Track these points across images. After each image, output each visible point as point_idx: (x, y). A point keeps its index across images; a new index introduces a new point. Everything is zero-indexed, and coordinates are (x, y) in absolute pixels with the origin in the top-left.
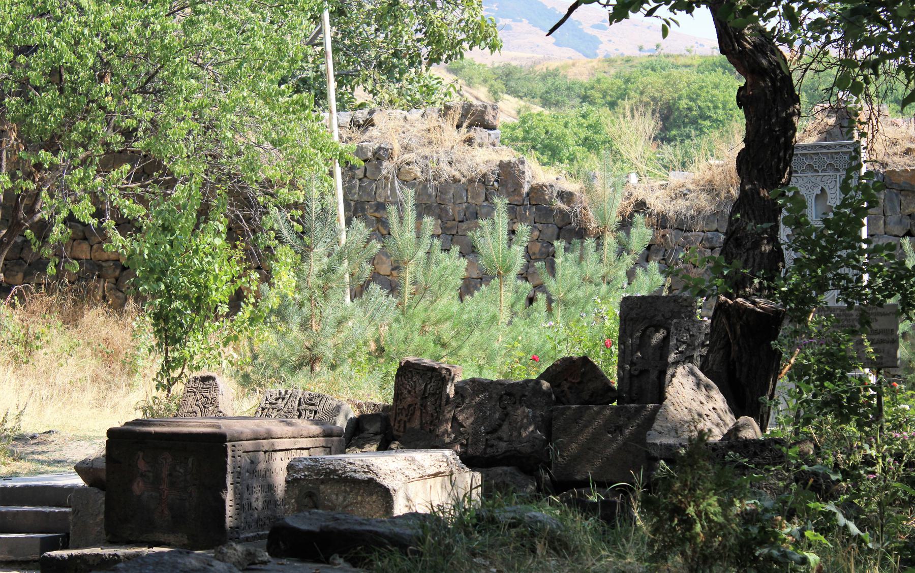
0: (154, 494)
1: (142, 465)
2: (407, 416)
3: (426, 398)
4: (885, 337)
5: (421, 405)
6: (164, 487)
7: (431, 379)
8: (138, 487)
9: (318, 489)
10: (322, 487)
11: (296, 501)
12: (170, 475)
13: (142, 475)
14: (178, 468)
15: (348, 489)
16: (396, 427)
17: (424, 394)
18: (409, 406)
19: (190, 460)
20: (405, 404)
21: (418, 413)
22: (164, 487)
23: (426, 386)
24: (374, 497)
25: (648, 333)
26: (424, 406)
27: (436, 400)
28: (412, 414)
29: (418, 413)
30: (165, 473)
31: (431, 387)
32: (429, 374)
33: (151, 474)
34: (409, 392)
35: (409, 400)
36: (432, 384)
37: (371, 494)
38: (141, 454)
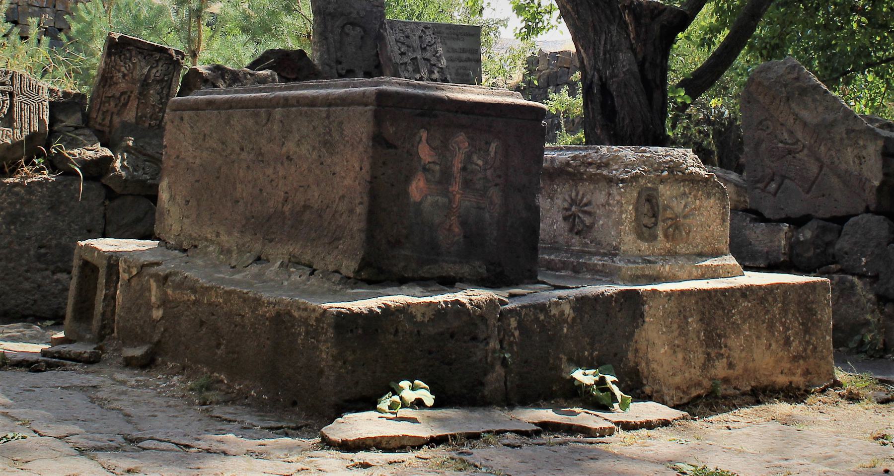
0: (441, 200)
1: (425, 153)
2: (116, 105)
3: (148, 85)
4: (471, 57)
5: (140, 94)
6: (456, 188)
7: (157, 61)
8: (417, 188)
9: (656, 190)
10: (661, 186)
11: (636, 209)
12: (464, 169)
13: (425, 170)
14: (475, 158)
15: (687, 191)
16: (99, 120)
17: (145, 80)
18: (123, 93)
19: (493, 145)
20: (114, 91)
21: (133, 104)
22: (456, 188)
23: (149, 70)
24: (712, 201)
25: (346, 30)
26: (143, 94)
27: (162, 88)
28: (125, 105)
29: (133, 104)
30: (457, 165)
31: (157, 72)
32: (157, 56)
33: (438, 167)
34: (124, 76)
35: (123, 86)
36: (160, 68)
37: (709, 196)
38: (424, 134)
